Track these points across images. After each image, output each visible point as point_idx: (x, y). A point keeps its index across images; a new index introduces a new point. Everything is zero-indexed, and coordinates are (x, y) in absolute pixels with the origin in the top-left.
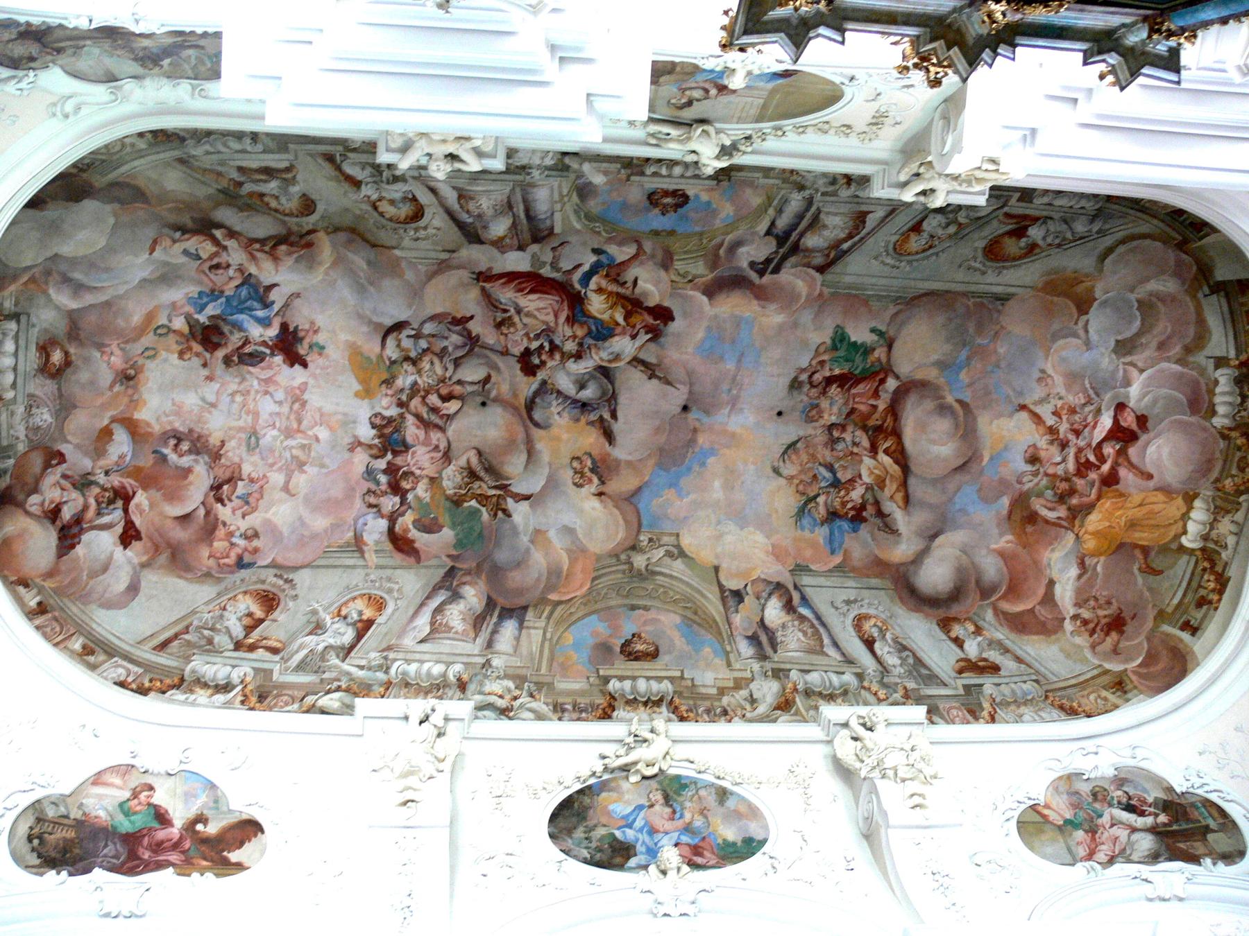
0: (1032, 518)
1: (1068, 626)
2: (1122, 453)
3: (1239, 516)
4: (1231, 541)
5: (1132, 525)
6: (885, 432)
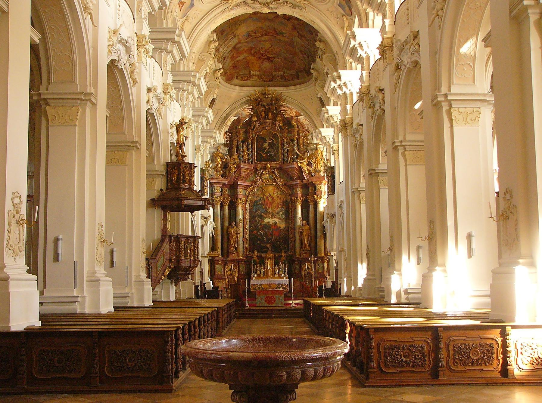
0: (251, 50)
4: (254, 79)
5: (253, 63)
6: (266, 35)
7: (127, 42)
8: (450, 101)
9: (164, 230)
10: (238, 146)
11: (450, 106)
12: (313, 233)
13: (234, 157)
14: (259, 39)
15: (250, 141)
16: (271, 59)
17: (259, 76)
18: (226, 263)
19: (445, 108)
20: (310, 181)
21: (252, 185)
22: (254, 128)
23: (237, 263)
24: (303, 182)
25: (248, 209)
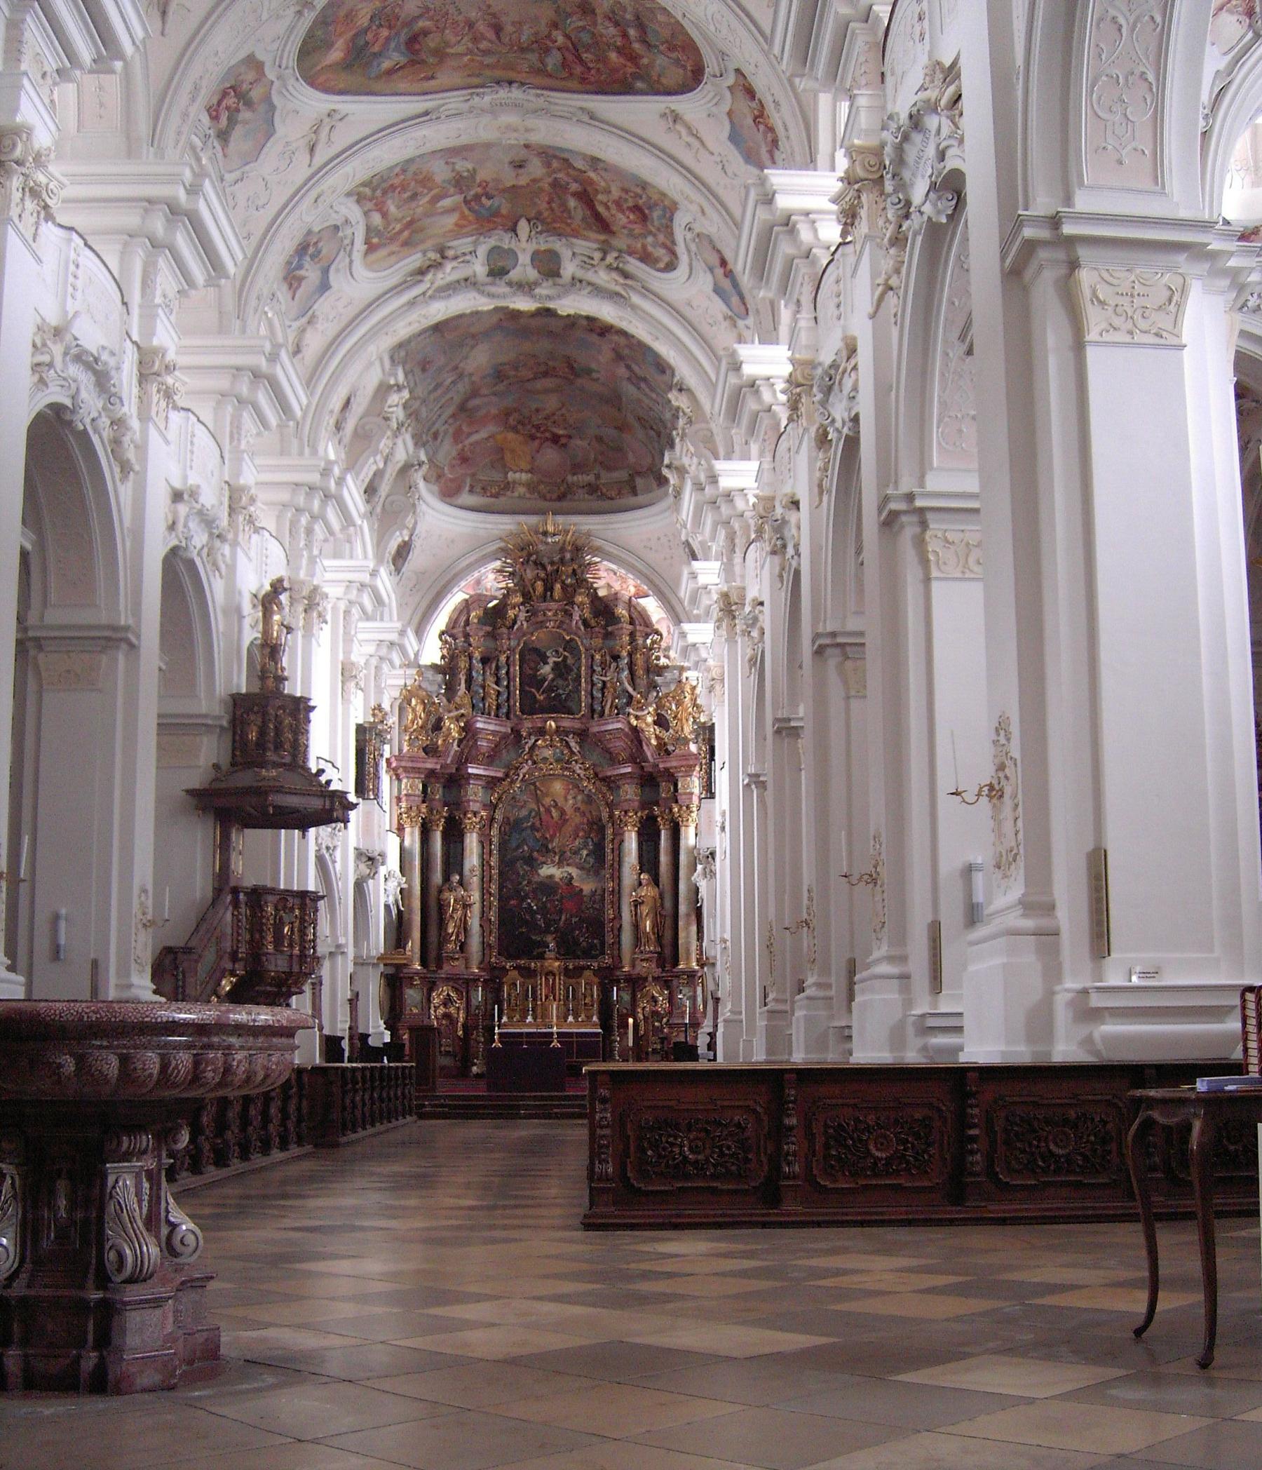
1: (460, 446)
2: (547, 439)
3: (528, 495)
4: (516, 494)
6: (546, 374)
7: (96, 360)
8: (922, 511)
9: (223, 876)
10: (470, 670)
11: (924, 525)
12: (668, 904)
13: (457, 699)
14: (529, 386)
15: (503, 659)
16: (563, 441)
17: (531, 487)
18: (434, 983)
19: (909, 530)
20: (661, 766)
21: (507, 775)
22: (515, 622)
23: (464, 985)
24: (642, 768)
25: (495, 840)
